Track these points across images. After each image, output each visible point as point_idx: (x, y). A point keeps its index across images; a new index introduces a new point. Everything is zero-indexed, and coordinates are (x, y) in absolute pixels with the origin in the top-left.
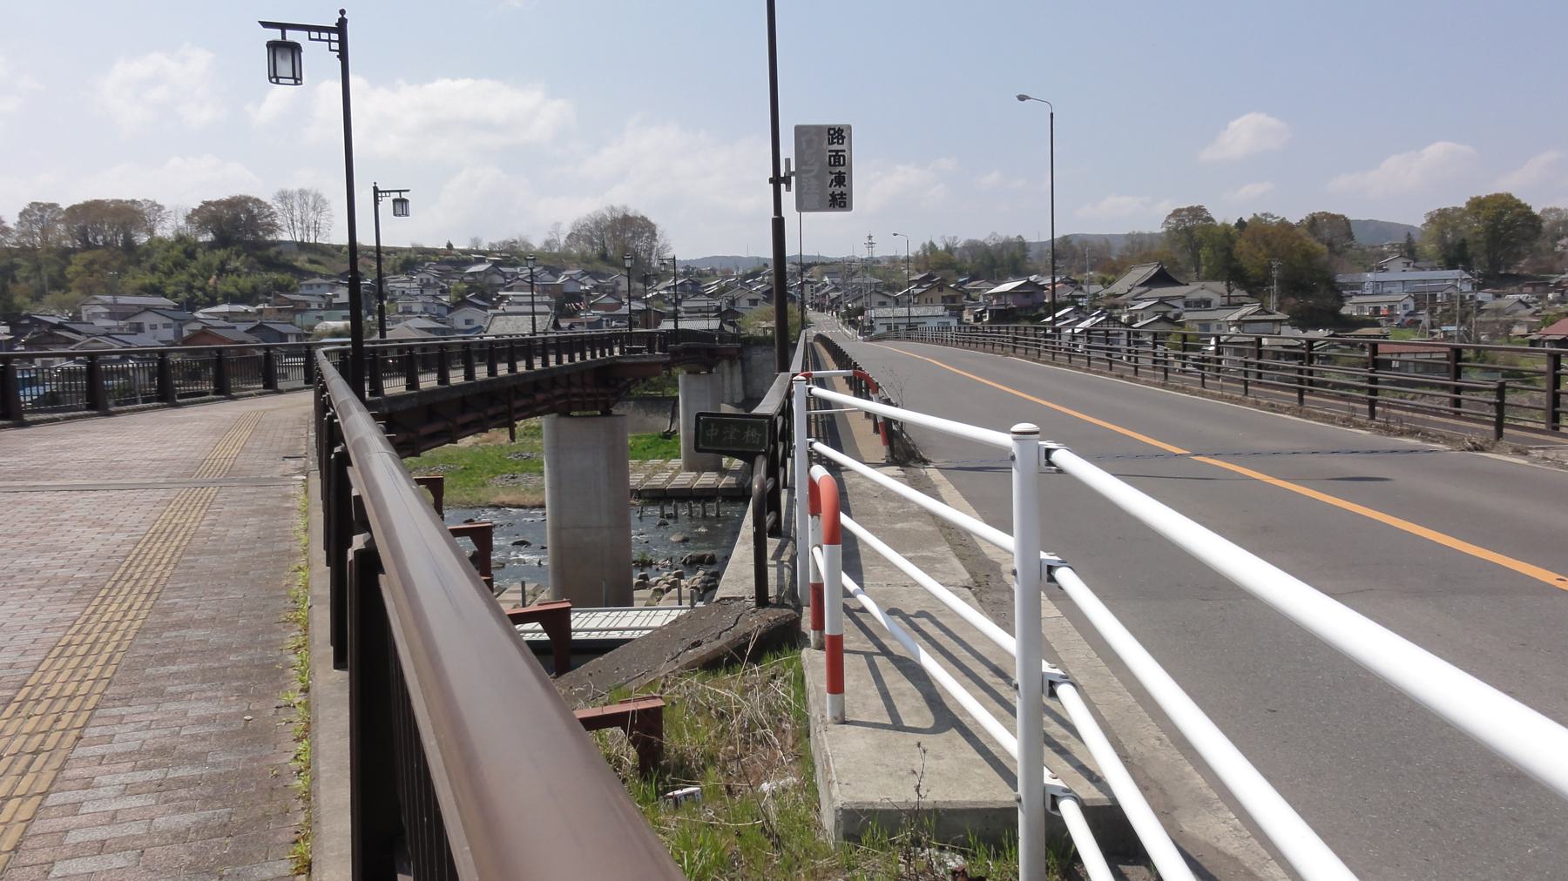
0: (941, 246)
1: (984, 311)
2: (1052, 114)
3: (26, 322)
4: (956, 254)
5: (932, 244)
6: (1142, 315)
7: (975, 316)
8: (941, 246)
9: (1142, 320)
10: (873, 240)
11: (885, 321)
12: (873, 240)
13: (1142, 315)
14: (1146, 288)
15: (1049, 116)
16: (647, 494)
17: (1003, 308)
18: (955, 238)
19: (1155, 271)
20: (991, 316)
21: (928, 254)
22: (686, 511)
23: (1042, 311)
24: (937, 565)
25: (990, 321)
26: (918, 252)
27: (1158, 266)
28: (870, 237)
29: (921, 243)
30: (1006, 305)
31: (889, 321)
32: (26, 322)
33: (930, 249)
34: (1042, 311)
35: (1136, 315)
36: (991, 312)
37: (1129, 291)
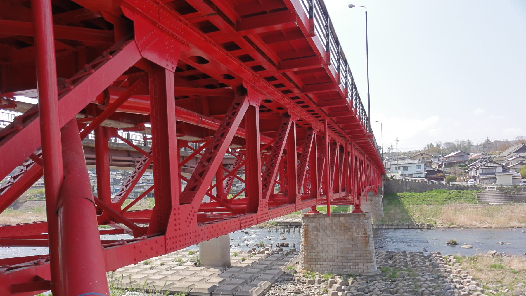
0: (435, 145)
1: (442, 164)
2: (366, 12)
3: (127, 174)
4: (441, 148)
5: (431, 145)
6: (511, 163)
7: (439, 166)
8: (435, 145)
9: (511, 164)
10: (398, 139)
11: (394, 166)
12: (398, 139)
13: (511, 163)
14: (516, 153)
15: (365, 13)
16: (284, 224)
17: (450, 162)
18: (441, 142)
19: (521, 146)
20: (445, 165)
21: (429, 148)
22: (293, 230)
23: (467, 163)
24: (489, 273)
25: (445, 167)
26: (425, 148)
27: (522, 144)
28: (397, 138)
29: (427, 144)
30: (451, 161)
31: (396, 166)
32: (127, 174)
33: (430, 145)
34: (467, 163)
35: (509, 163)
36: (445, 164)
37: (509, 155)
